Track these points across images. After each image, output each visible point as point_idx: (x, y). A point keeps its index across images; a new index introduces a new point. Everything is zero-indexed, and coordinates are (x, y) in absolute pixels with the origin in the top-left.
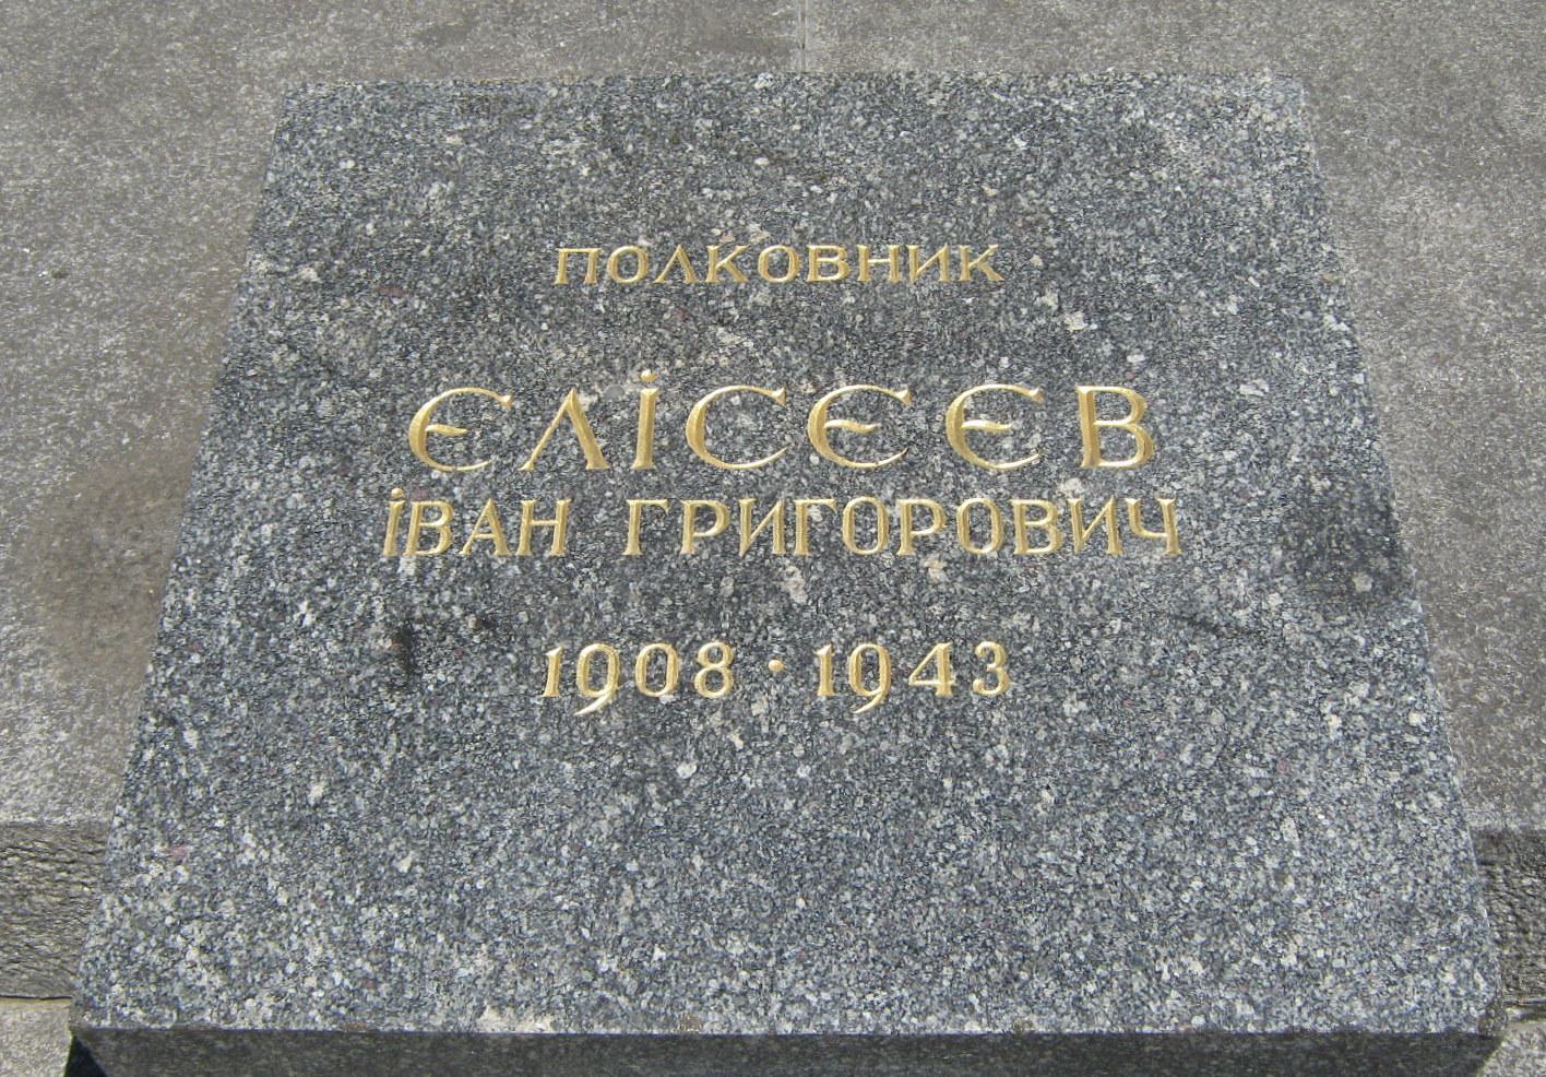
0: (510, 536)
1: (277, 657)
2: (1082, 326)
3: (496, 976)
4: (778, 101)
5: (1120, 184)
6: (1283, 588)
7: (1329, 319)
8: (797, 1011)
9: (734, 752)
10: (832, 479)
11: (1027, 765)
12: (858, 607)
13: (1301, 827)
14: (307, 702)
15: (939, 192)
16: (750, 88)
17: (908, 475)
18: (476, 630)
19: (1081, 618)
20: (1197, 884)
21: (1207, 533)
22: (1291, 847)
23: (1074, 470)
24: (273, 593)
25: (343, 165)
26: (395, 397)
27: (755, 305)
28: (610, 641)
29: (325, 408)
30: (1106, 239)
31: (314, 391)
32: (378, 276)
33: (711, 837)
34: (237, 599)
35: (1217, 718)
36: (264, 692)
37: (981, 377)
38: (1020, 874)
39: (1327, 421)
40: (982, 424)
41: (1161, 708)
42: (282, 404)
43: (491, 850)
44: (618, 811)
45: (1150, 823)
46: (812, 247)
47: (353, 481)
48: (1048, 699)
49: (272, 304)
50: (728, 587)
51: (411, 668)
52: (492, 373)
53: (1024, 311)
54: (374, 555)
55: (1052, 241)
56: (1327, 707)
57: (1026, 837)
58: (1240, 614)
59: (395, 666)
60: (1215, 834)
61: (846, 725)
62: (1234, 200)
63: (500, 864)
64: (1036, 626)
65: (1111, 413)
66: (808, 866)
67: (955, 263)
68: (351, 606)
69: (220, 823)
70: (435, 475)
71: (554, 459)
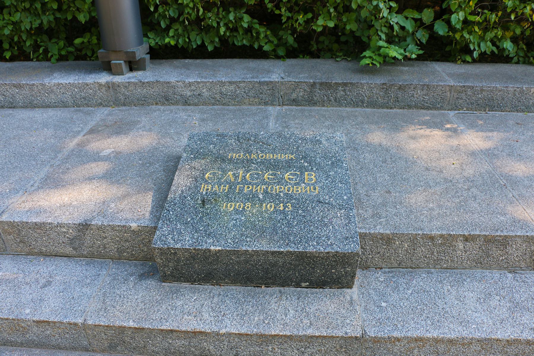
3: (213, 242)
8: (256, 247)
17: (279, 183)
23: (304, 183)
29: (193, 173)
35: (322, 214)
37: (291, 171)
40: (291, 177)
45: (310, 226)
50: (251, 196)
51: (204, 205)
65: (310, 176)
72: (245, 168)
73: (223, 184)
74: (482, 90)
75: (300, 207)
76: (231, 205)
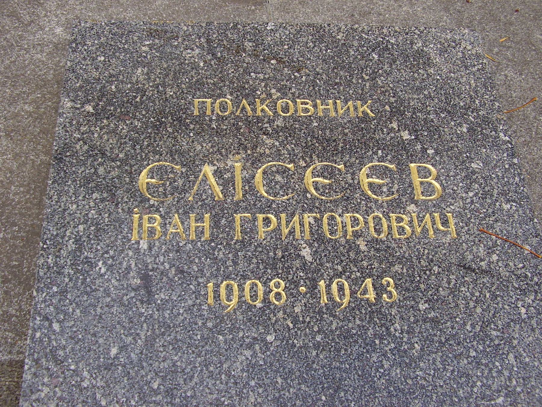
0: (187, 229)
1: (91, 288)
2: (409, 137)
4: (278, 35)
5: (416, 75)
6: (498, 252)
7: (501, 134)
9: (289, 329)
10: (317, 204)
11: (408, 332)
12: (333, 262)
13: (516, 357)
14: (106, 309)
15: (346, 77)
16: (266, 29)
18: (176, 275)
19: (422, 266)
20: (479, 384)
21: (466, 228)
22: (513, 366)
24: (86, 258)
25: (99, 58)
26: (131, 166)
27: (277, 126)
28: (234, 279)
29: (101, 171)
30: (413, 99)
31: (96, 163)
32: (119, 110)
33: (284, 369)
34: (71, 260)
35: (479, 310)
36: (86, 304)
38: (410, 382)
39: (506, 179)
41: (457, 305)
42: (83, 169)
43: (193, 377)
44: (244, 358)
46: (298, 100)
47: (117, 205)
48: (413, 303)
49: (74, 122)
50: (280, 254)
51: (149, 293)
52: (171, 156)
53: (385, 130)
54: (130, 240)
55: (392, 100)
56: (520, 304)
57: (411, 365)
58: (482, 263)
59: (143, 292)
60: (484, 361)
61: (335, 316)
62: (460, 83)
63: (196, 384)
64: (405, 271)
65: (425, 176)
66: (325, 381)
67: (356, 108)
68: (121, 263)
69: (73, 367)
70: (152, 202)
71: (201, 195)
72: (245, 149)
73: (192, 208)
75: (418, 288)
76: (229, 288)
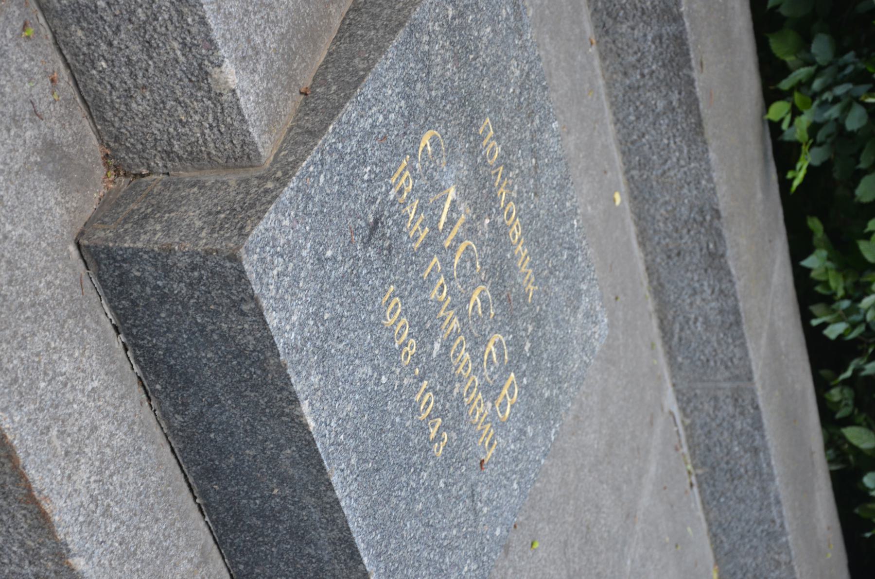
55: (544, 307)
56: (468, 562)
74: (756, 451)
